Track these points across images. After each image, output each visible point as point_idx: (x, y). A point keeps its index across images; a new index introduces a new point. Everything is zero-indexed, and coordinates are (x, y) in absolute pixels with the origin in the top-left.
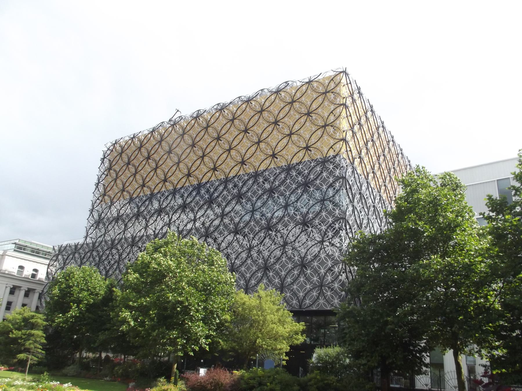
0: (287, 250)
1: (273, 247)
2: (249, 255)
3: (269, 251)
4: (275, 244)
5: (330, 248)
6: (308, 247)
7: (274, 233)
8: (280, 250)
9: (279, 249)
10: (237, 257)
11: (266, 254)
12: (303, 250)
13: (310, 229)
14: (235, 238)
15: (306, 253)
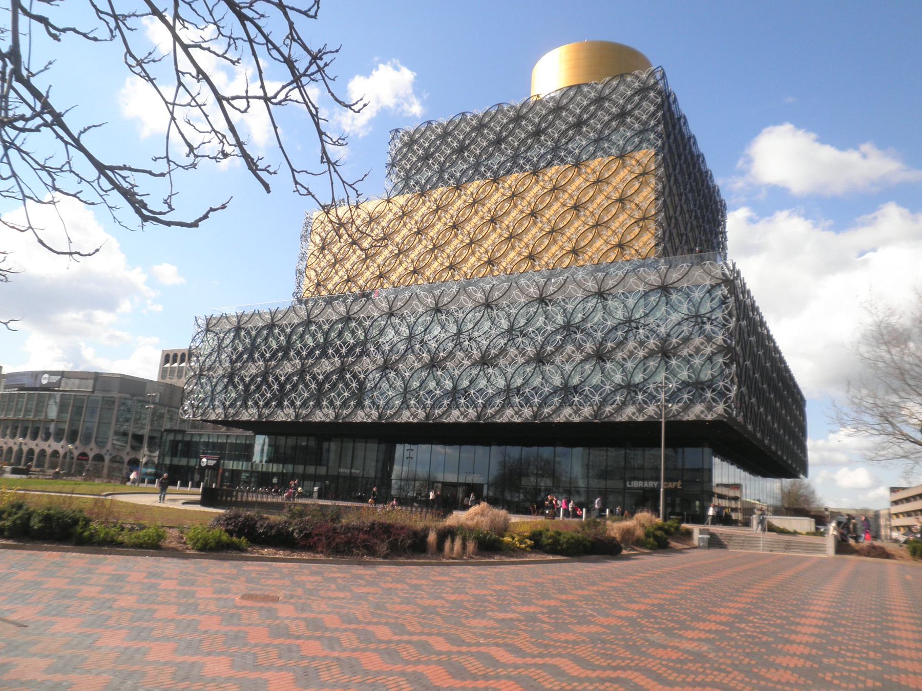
0: (462, 340)
1: (442, 335)
2: (409, 346)
3: (437, 341)
4: (445, 332)
5: (520, 339)
6: (491, 338)
7: (444, 317)
8: (453, 341)
9: (451, 338)
10: (392, 348)
11: (433, 345)
12: (484, 342)
13: (495, 312)
14: (389, 322)
15: (489, 345)
